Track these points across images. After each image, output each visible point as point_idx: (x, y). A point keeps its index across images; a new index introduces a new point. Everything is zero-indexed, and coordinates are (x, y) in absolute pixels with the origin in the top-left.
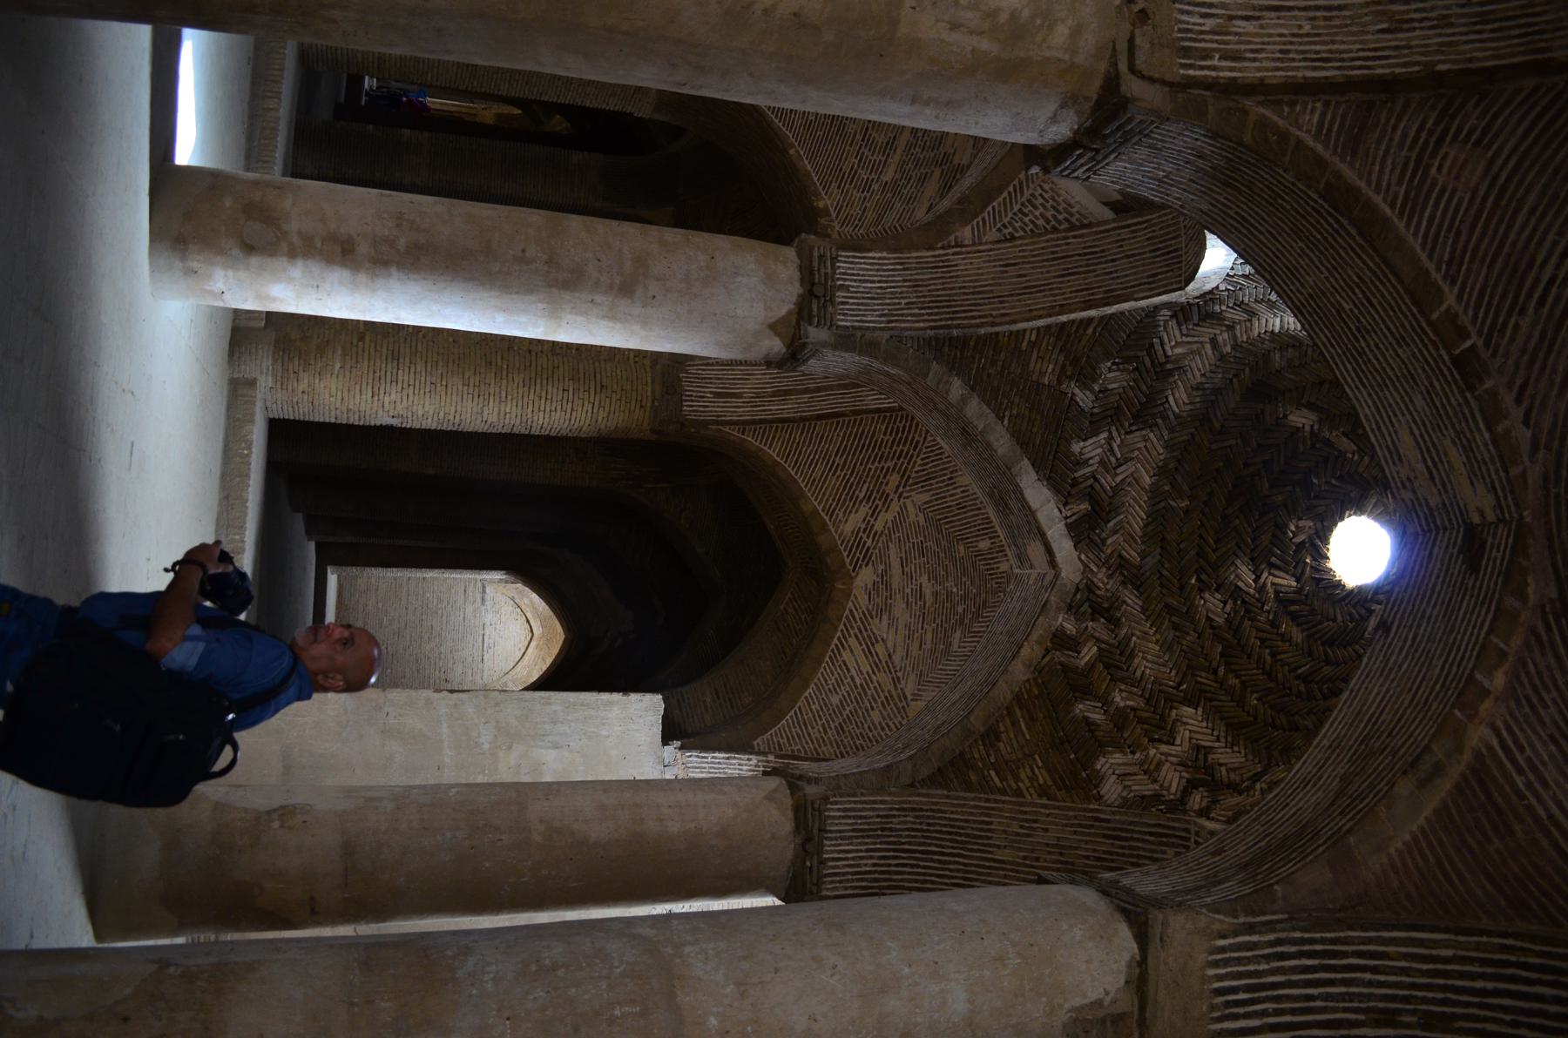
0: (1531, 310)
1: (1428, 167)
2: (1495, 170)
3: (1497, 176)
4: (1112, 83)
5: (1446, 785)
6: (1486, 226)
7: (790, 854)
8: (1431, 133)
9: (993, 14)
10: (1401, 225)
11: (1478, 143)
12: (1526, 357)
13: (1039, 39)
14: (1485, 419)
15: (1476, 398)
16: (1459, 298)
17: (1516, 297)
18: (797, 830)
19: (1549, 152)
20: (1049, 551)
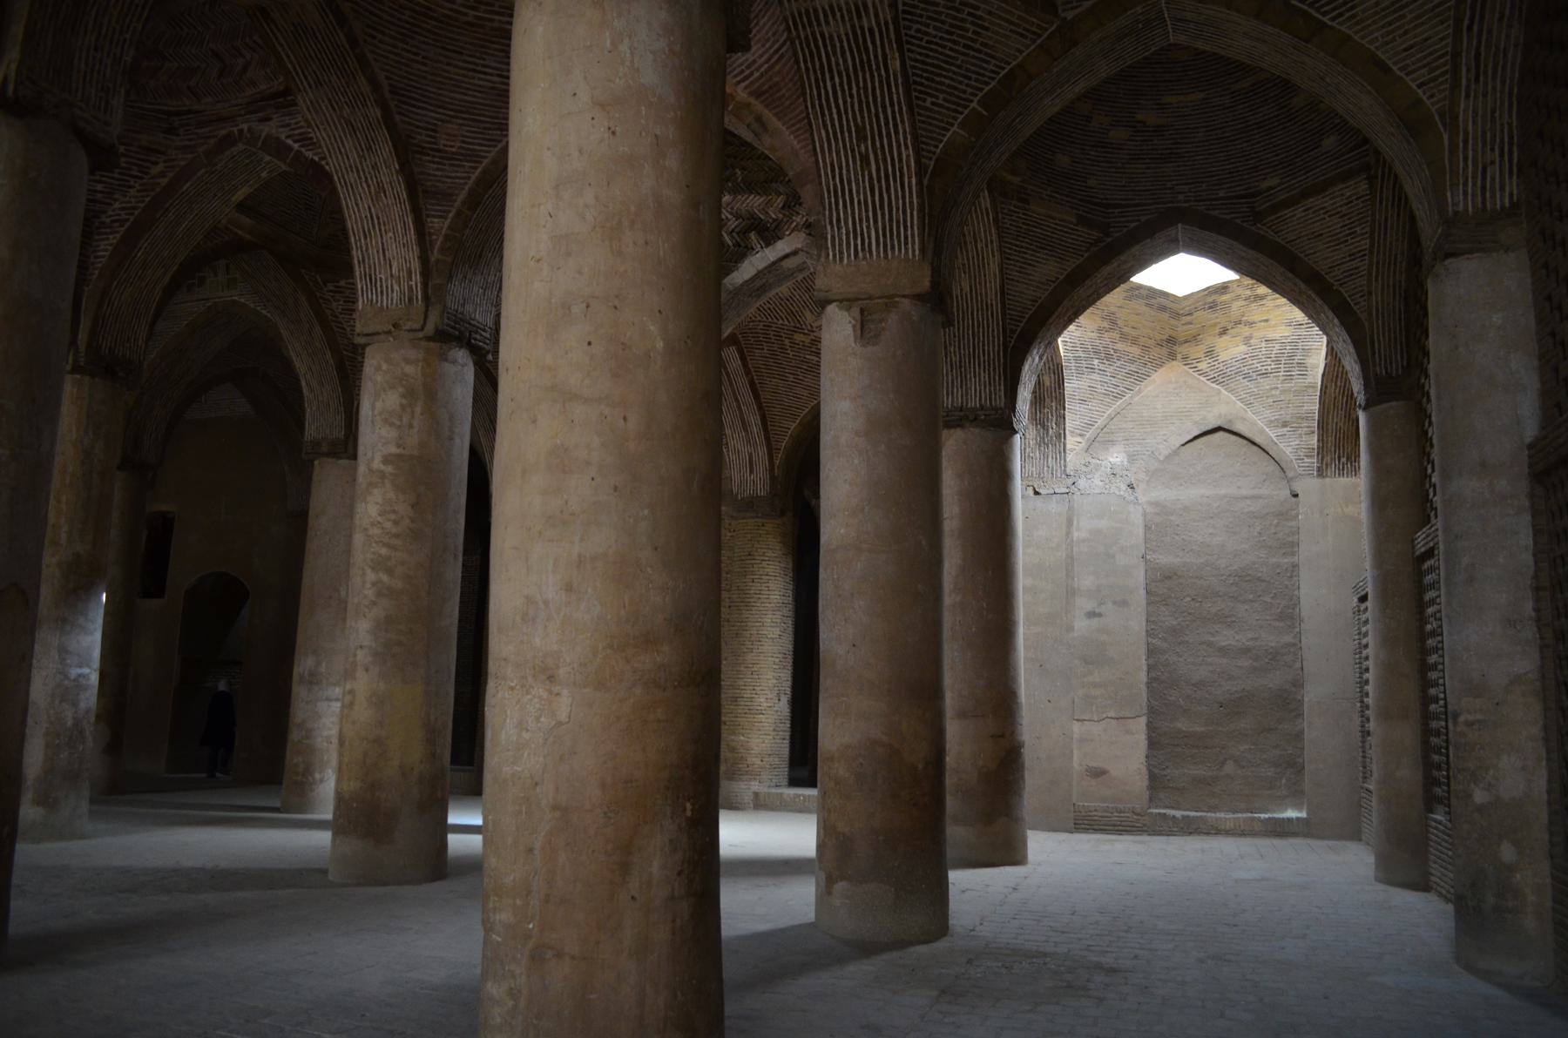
4: (428, 339)
5: (767, 115)
7: (977, 430)
9: (403, 407)
10: (486, 161)
18: (961, 426)
20: (786, 256)
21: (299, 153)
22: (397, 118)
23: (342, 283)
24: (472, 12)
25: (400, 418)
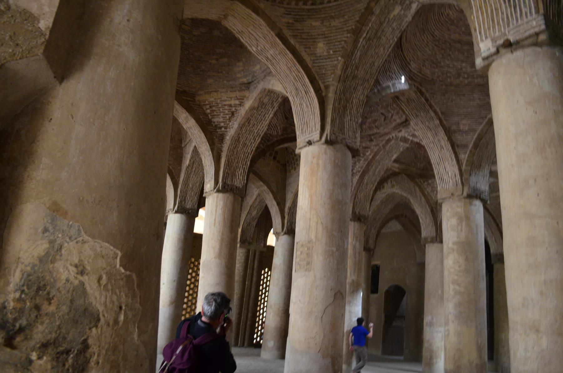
4: (465, 198)
9: (458, 224)
21: (412, 141)
22: (445, 122)
23: (430, 181)
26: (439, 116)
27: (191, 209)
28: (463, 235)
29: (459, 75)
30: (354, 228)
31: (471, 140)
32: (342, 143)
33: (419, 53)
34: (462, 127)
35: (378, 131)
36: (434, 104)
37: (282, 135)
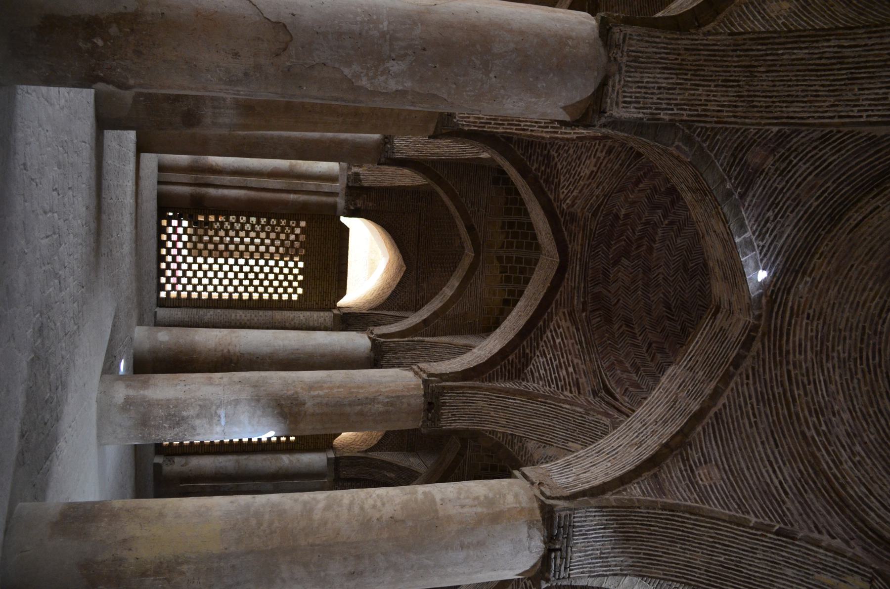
0: (786, 499)
1: (697, 482)
2: (721, 467)
3: (724, 468)
6: (739, 487)
8: (686, 470)
9: (477, 498)
11: (706, 462)
12: (804, 516)
13: (502, 502)
14: (812, 544)
15: (800, 539)
16: (757, 516)
17: (776, 500)
19: (731, 446)
22: (699, 429)
24: (813, 431)
25: (468, 497)
26: (710, 408)
27: (393, 147)
28: (452, 510)
29: (818, 412)
30: (412, 396)
31: (679, 494)
32: (609, 60)
33: (832, 293)
34: (701, 472)
35: (618, 396)
36: (732, 385)
37: (562, 212)
